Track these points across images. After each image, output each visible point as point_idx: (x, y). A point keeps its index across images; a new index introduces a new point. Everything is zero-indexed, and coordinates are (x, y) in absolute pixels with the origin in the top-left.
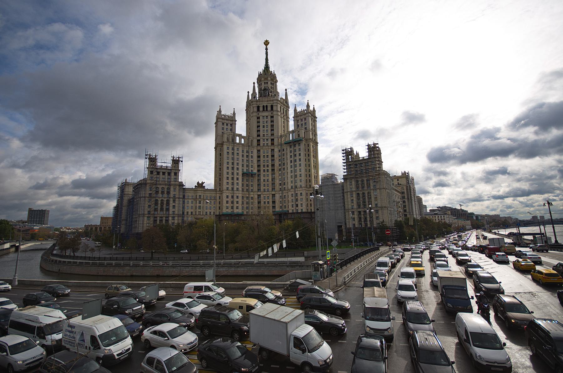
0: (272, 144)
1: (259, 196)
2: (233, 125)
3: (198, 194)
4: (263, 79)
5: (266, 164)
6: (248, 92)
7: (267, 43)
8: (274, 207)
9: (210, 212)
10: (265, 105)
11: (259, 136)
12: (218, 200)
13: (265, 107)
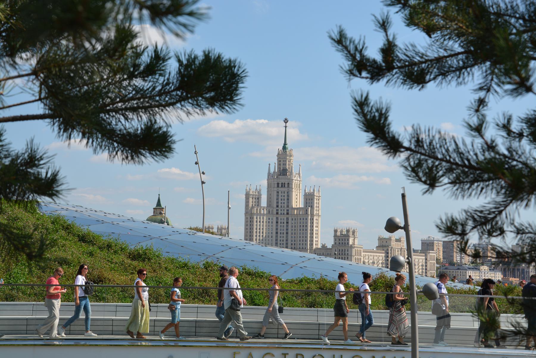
0: (288, 214)
2: (259, 199)
5: (282, 228)
6: (269, 164)
7: (286, 121)
11: (277, 206)
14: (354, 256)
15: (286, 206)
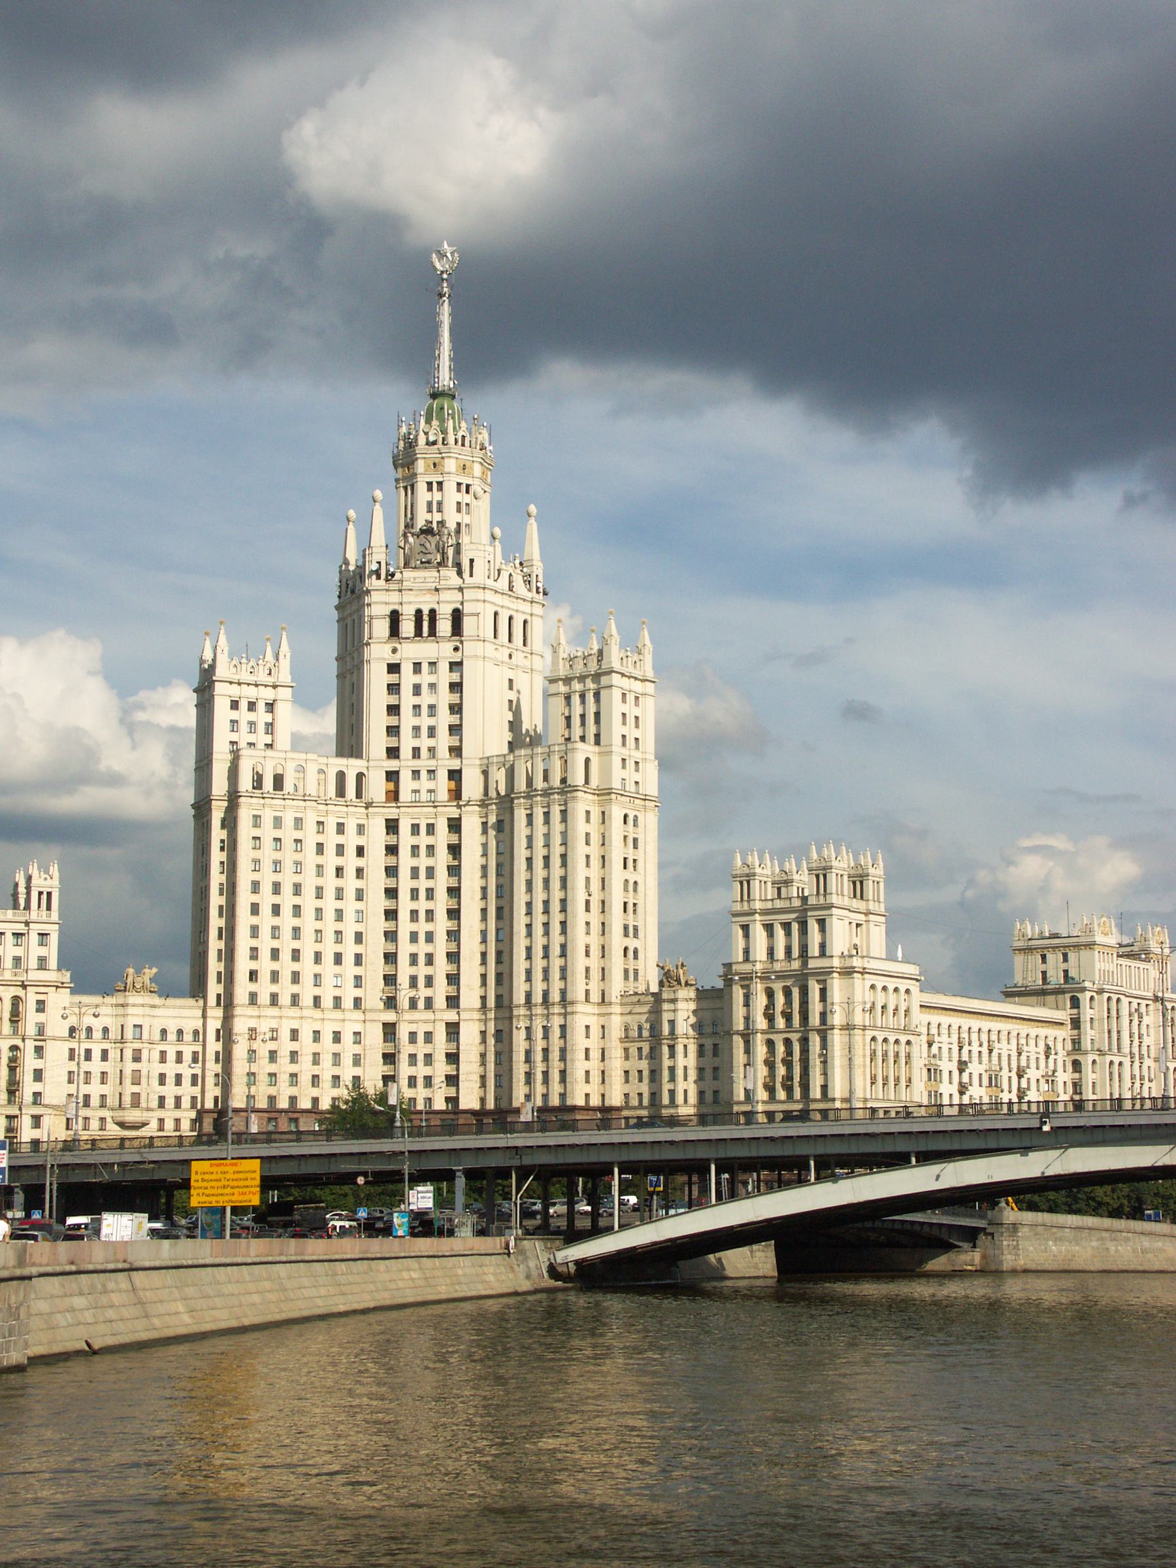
0: (456, 794)
1: (390, 1030)
3: (130, 1022)
4: (420, 466)
8: (452, 1080)
9: (178, 1100)
10: (426, 612)
11: (393, 753)
12: (214, 1046)
13: (426, 617)
14: (864, 1028)
15: (443, 752)
